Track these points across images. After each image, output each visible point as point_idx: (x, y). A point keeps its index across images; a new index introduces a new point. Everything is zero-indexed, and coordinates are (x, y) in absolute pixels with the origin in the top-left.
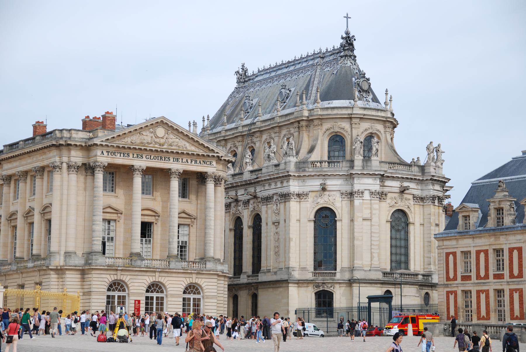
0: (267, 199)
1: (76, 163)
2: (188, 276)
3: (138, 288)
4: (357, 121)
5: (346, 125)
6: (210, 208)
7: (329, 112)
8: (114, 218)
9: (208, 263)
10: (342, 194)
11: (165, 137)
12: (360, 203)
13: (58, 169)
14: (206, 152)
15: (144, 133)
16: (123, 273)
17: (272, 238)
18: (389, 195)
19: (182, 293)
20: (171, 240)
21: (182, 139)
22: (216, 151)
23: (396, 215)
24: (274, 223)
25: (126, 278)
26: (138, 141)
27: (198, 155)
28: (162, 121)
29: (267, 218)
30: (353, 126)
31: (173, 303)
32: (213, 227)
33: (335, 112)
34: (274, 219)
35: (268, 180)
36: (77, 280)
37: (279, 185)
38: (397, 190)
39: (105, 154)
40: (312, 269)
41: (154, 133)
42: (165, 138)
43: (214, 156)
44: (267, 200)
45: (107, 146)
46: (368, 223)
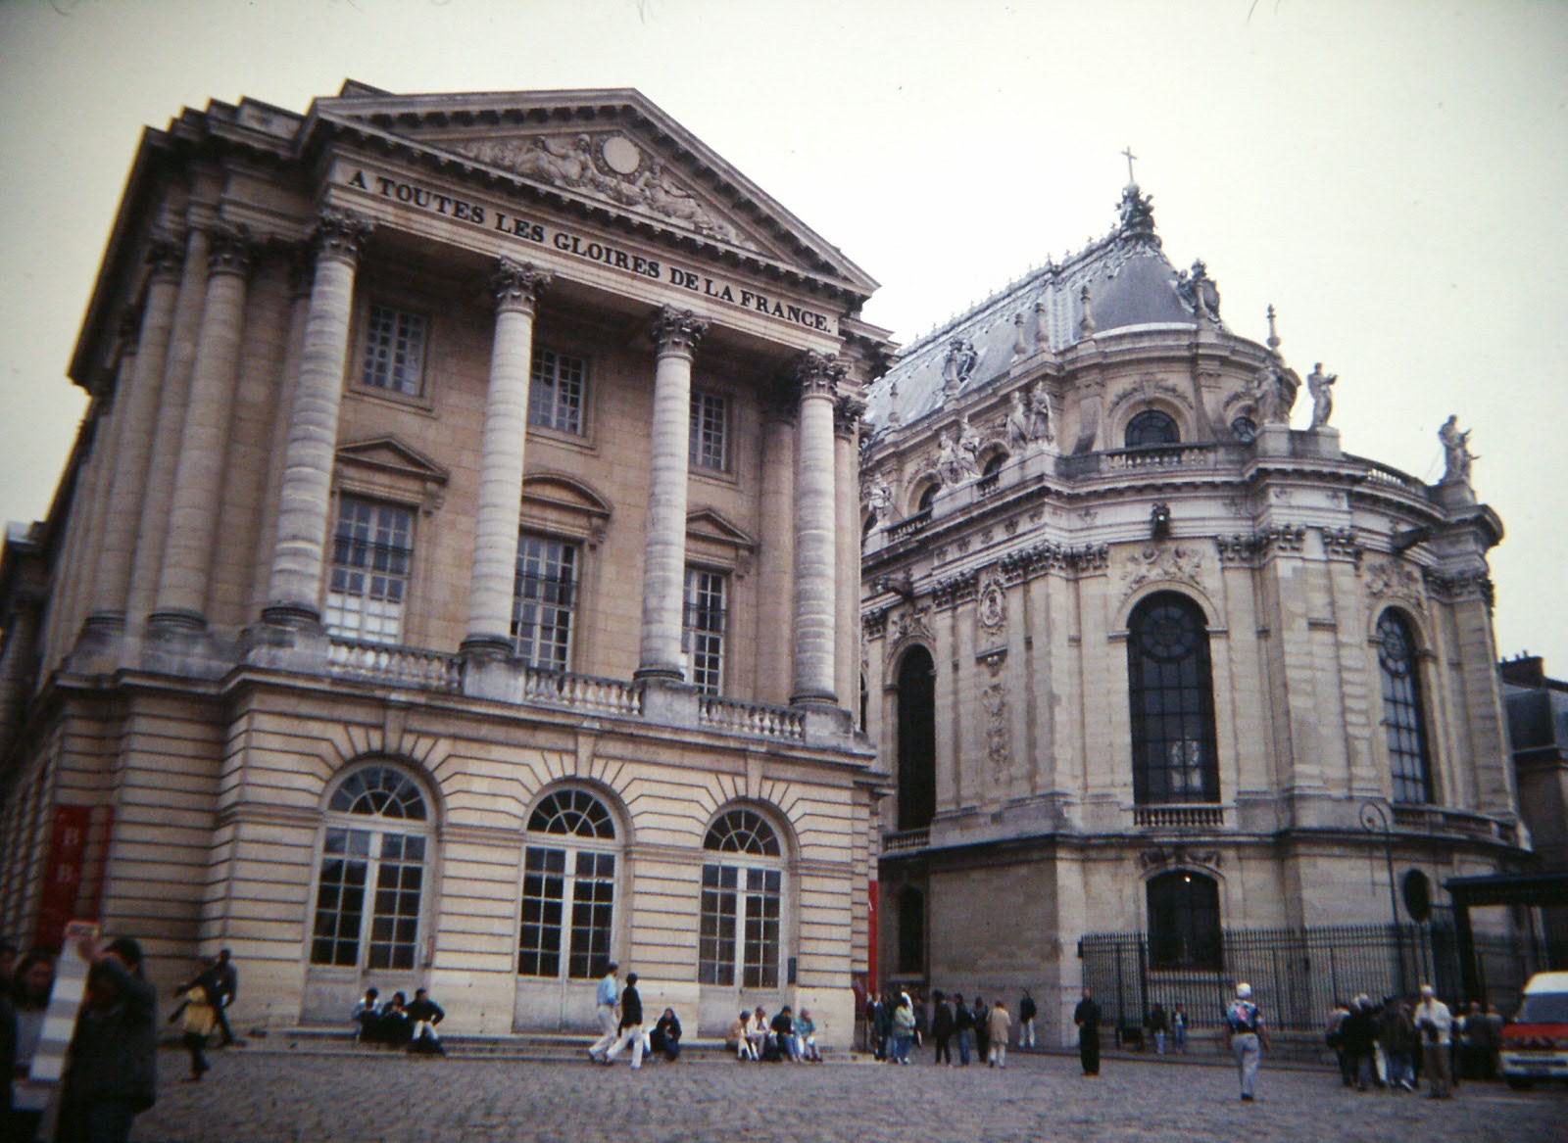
0: (955, 592)
2: (727, 763)
4: (1211, 366)
5: (1179, 379)
6: (818, 493)
7: (1126, 345)
8: (408, 498)
9: (810, 717)
10: (1222, 546)
11: (641, 182)
12: (1294, 570)
14: (804, 269)
16: (416, 723)
18: (1369, 559)
19: (698, 842)
20: (653, 602)
22: (841, 271)
23: (1387, 626)
24: (981, 660)
27: (772, 273)
29: (955, 650)
30: (1203, 381)
31: (655, 886)
32: (831, 571)
33: (1146, 343)
35: (958, 527)
37: (999, 534)
38: (1382, 543)
40: (1127, 798)
41: (597, 152)
44: (953, 594)
45: (375, 143)
46: (1324, 637)
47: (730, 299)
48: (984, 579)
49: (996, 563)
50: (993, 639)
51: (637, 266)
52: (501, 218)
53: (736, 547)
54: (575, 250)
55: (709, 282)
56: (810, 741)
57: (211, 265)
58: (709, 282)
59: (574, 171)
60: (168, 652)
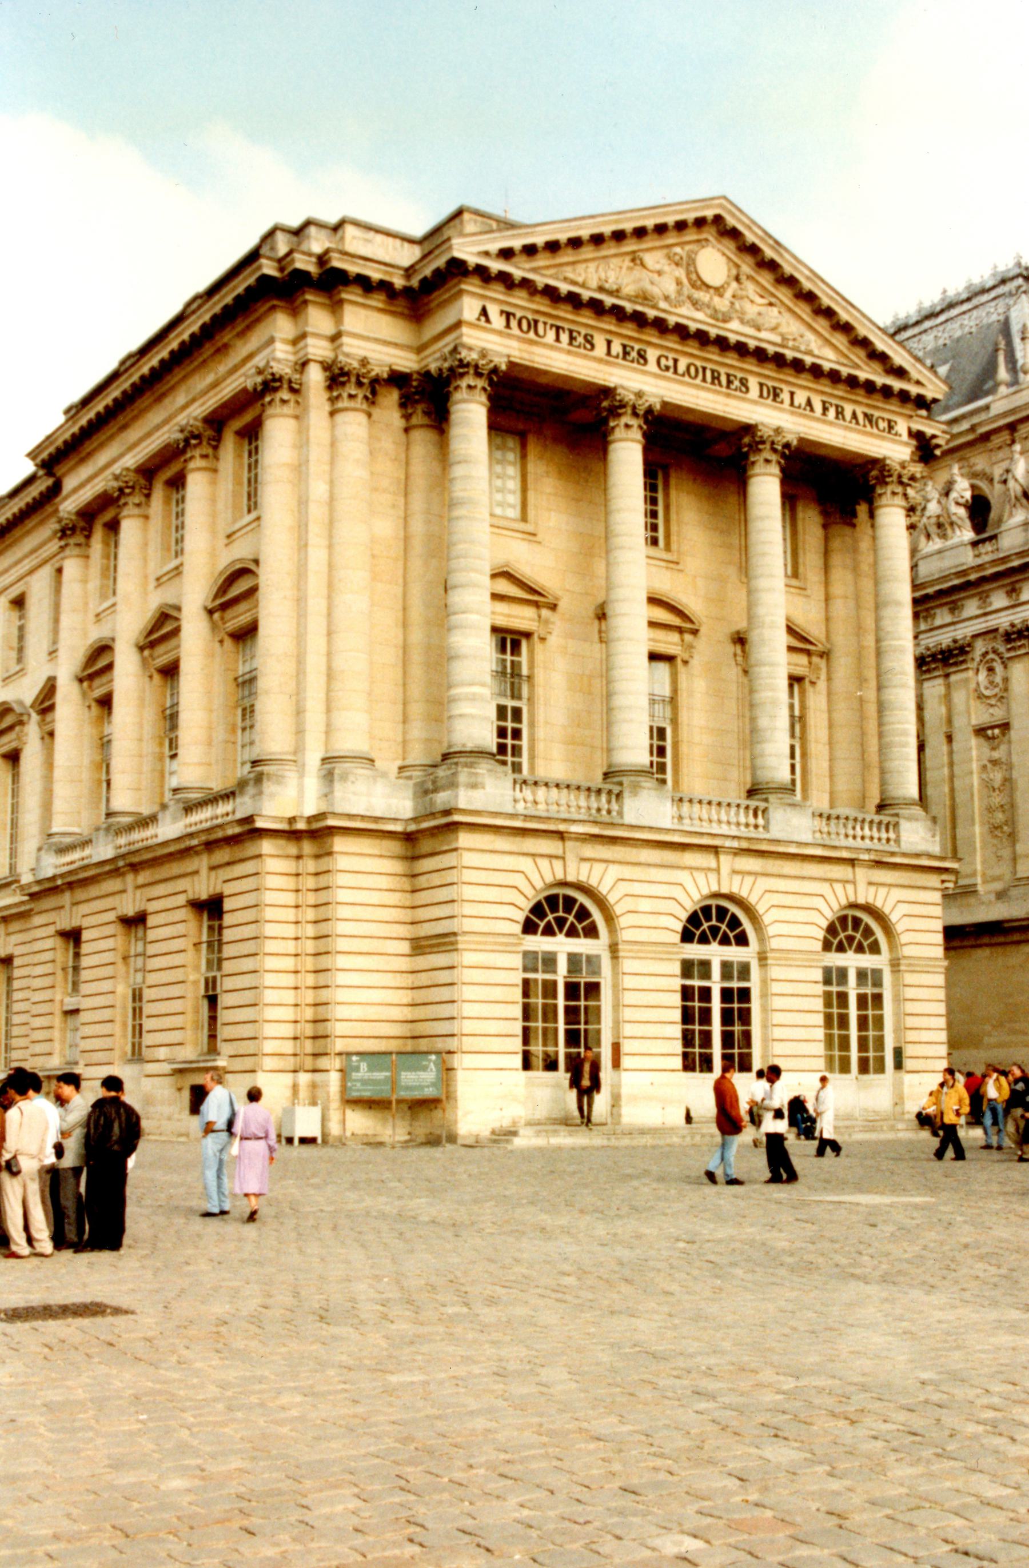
1: (364, 362)
3: (650, 921)
9: (905, 826)
13: (285, 394)
15: (649, 259)
16: (590, 850)
17: (976, 780)
21: (790, 310)
22: (914, 375)
24: (980, 731)
25: (604, 874)
26: (629, 290)
27: (852, 382)
28: (718, 219)
31: (788, 988)
34: (980, 715)
36: (384, 882)
37: (999, 600)
39: (497, 321)
42: (728, 294)
43: (904, 397)
45: (505, 279)
47: (812, 410)
48: (980, 647)
49: (996, 630)
50: (991, 711)
51: (729, 382)
52: (609, 343)
53: (808, 653)
54: (676, 372)
55: (792, 394)
56: (905, 847)
57: (332, 400)
58: (792, 394)
59: (671, 288)
60: (355, 794)
